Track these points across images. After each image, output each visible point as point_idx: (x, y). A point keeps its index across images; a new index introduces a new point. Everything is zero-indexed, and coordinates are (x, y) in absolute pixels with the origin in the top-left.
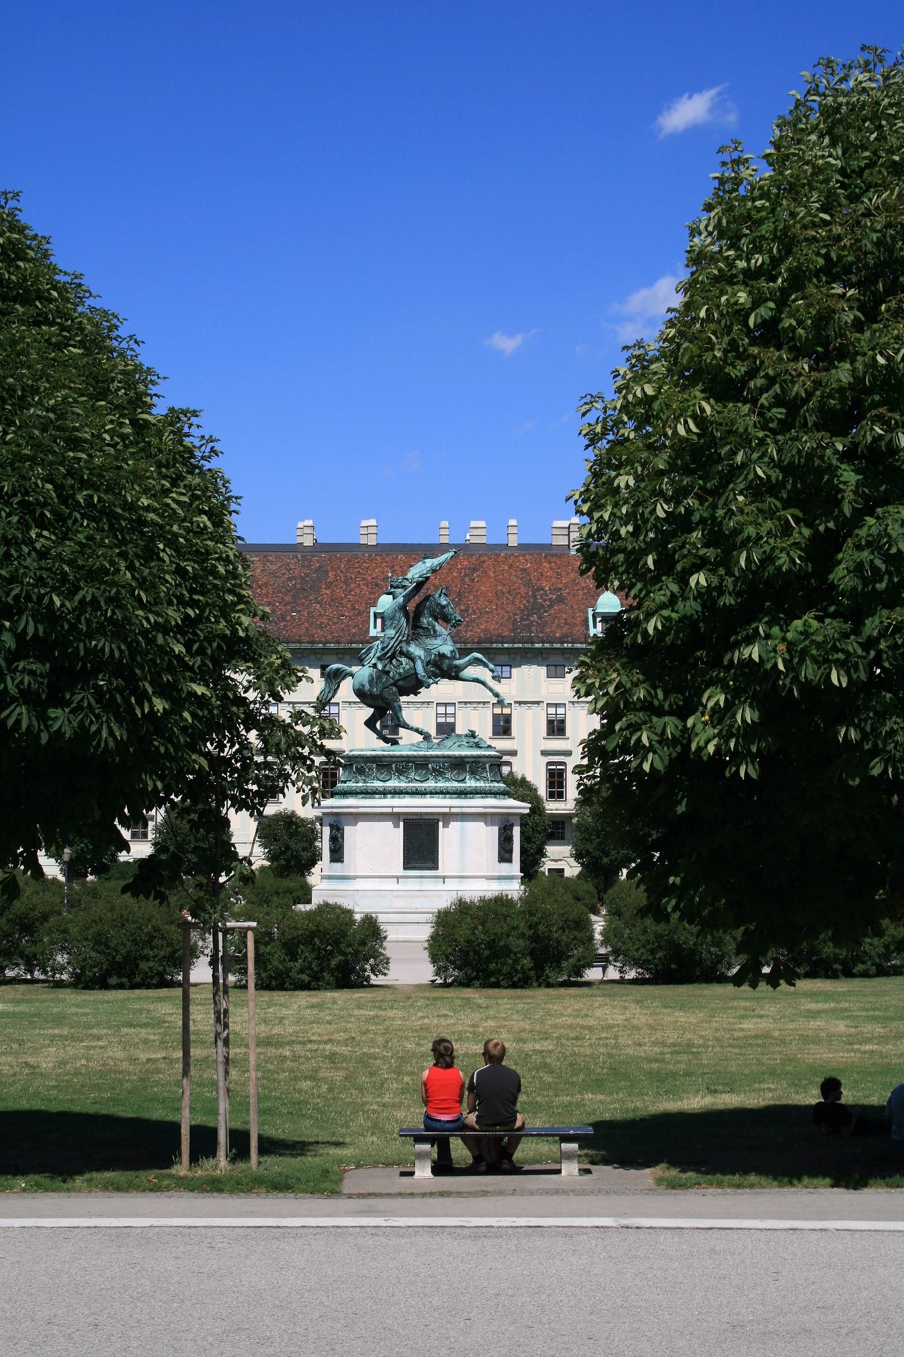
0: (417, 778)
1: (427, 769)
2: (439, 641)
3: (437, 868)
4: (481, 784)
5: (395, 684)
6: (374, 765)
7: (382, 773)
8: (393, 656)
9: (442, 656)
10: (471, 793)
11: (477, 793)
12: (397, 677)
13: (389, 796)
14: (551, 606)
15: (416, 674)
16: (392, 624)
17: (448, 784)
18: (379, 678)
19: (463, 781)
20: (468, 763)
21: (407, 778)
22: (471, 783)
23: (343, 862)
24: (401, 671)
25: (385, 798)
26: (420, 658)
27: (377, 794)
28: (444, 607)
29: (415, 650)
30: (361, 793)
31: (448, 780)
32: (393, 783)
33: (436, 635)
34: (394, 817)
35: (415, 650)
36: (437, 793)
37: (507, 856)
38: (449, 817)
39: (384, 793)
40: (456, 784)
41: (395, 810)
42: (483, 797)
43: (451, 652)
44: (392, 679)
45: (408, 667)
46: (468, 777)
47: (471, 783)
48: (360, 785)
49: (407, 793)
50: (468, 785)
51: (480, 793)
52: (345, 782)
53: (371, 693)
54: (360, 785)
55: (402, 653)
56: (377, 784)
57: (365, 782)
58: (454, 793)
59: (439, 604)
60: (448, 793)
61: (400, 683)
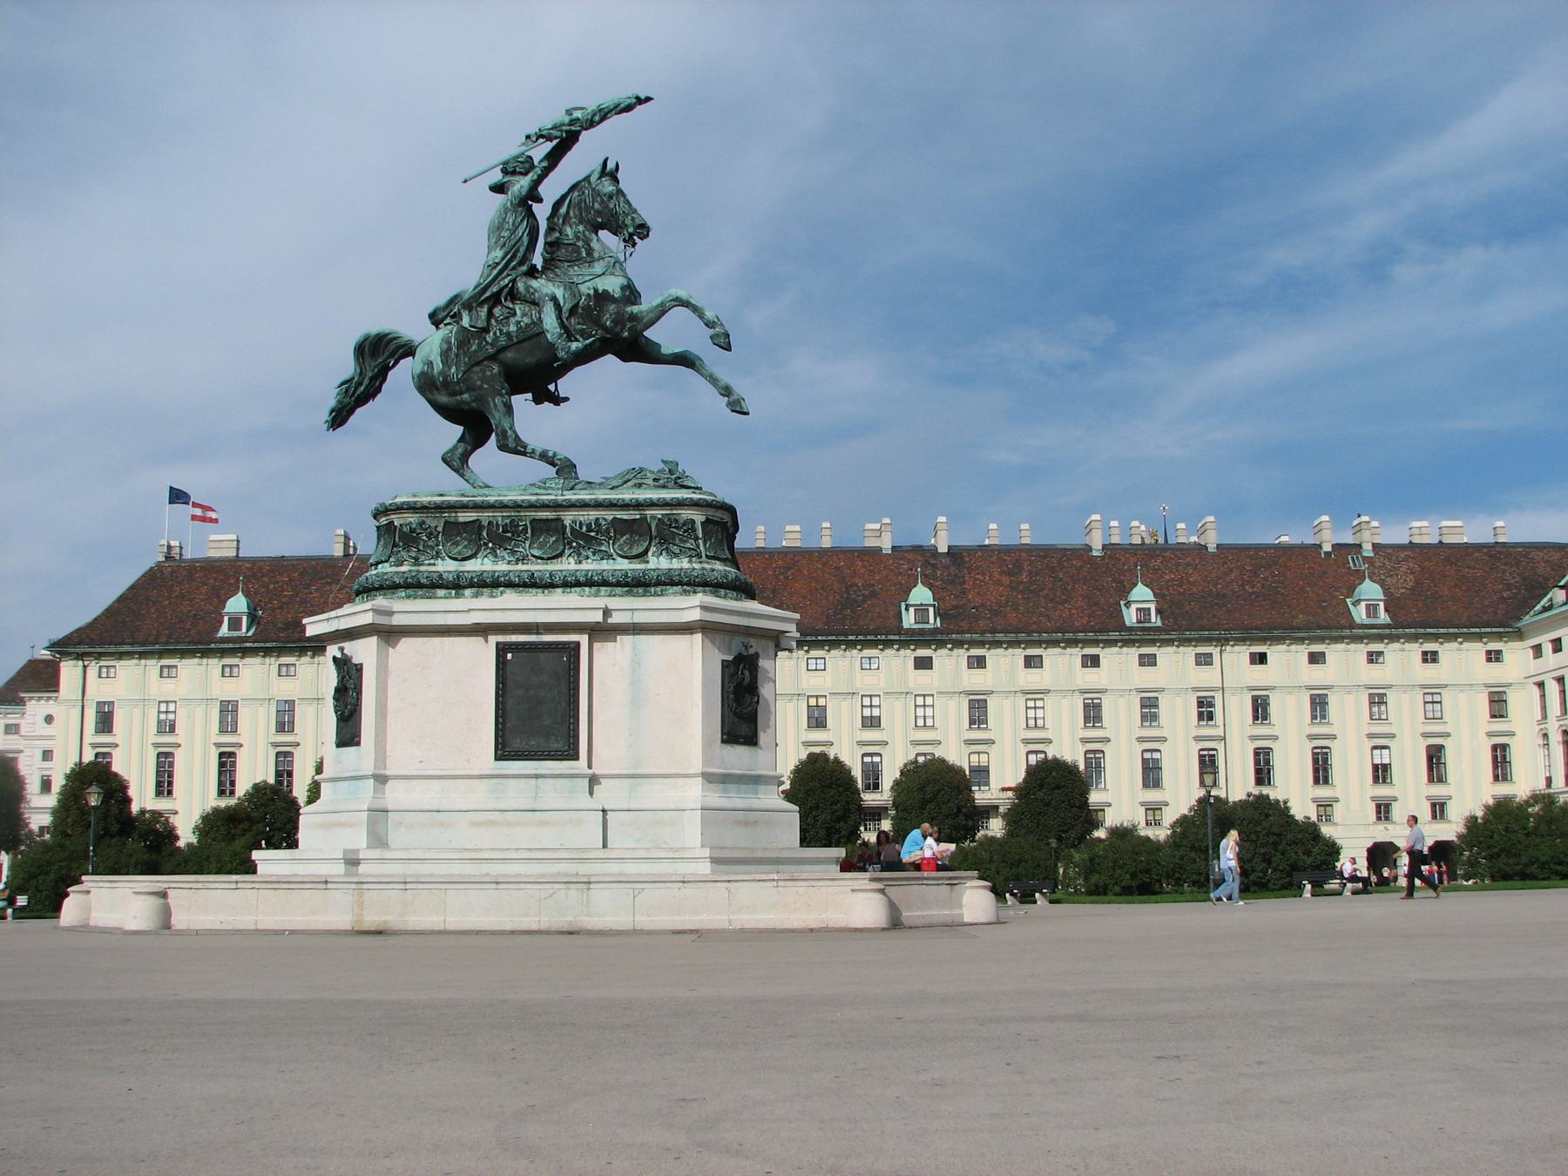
0: (537, 553)
4: (685, 564)
7: (456, 544)
9: (602, 297)
10: (659, 583)
11: (673, 584)
12: (503, 341)
13: (468, 592)
15: (542, 333)
17: (605, 565)
19: (642, 556)
21: (513, 552)
22: (659, 562)
23: (358, 744)
24: (513, 328)
25: (458, 596)
26: (554, 299)
27: (441, 587)
30: (407, 586)
32: (481, 565)
36: (578, 584)
37: (744, 729)
39: (457, 585)
40: (623, 565)
43: (623, 288)
45: (526, 320)
46: (653, 549)
47: (659, 562)
48: (404, 568)
49: (510, 585)
50: (651, 566)
51: (680, 583)
53: (445, 377)
54: (404, 568)
56: (446, 566)
57: (417, 562)
58: (618, 584)
60: (605, 583)
61: (509, 355)
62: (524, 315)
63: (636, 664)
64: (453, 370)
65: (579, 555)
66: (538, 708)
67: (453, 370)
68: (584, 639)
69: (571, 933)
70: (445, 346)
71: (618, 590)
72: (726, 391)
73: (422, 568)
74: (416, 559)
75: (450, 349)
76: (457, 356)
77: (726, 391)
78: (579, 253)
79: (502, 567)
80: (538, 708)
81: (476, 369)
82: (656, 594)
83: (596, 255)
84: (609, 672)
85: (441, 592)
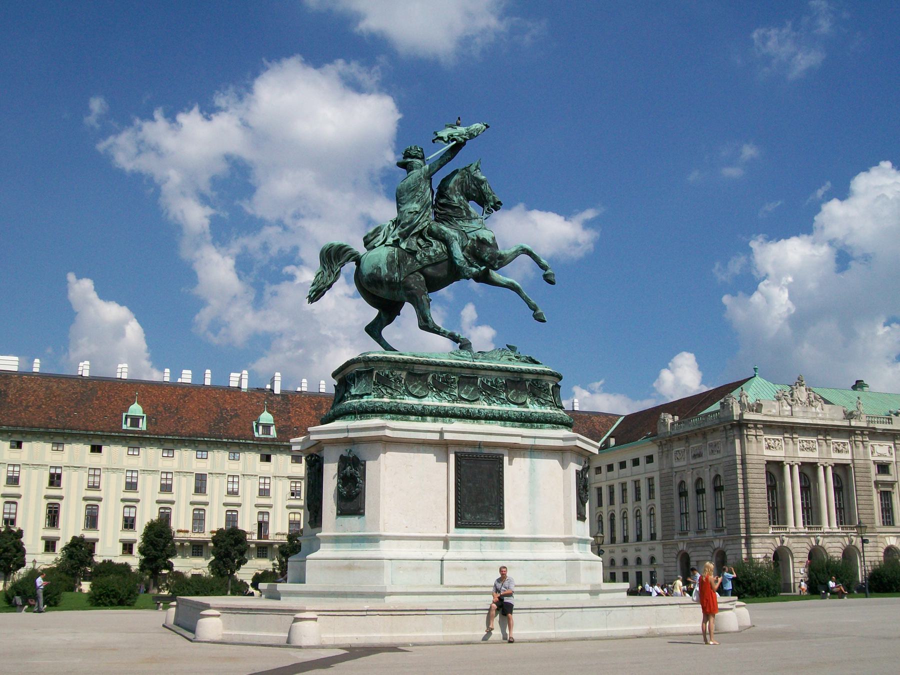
0: (463, 396)
1: (476, 384)
2: (475, 224)
3: (501, 526)
5: (421, 271)
6: (404, 375)
7: (415, 387)
8: (420, 234)
9: (482, 242)
12: (426, 262)
13: (429, 418)
14: (231, 419)
16: (414, 197)
18: (402, 260)
19: (523, 404)
20: (528, 380)
21: (450, 395)
22: (534, 408)
23: (363, 514)
24: (432, 254)
25: (424, 421)
28: (482, 182)
31: (504, 402)
32: (431, 401)
33: (469, 217)
34: (441, 446)
38: (516, 450)
39: (423, 414)
40: (515, 408)
41: (447, 436)
42: (553, 428)
44: (420, 263)
45: (439, 250)
47: (534, 408)
51: (550, 422)
52: (361, 396)
54: (386, 400)
55: (431, 233)
59: (476, 179)
62: (438, 246)
63: (532, 471)
64: (396, 275)
65: (489, 400)
66: (479, 496)
67: (396, 275)
68: (505, 452)
69: (640, 637)
70: (390, 259)
71: (517, 424)
72: (534, 308)
73: (398, 401)
74: (391, 394)
75: (393, 261)
76: (399, 266)
77: (534, 308)
78: (462, 213)
79: (446, 404)
80: (479, 496)
81: (411, 276)
82: (537, 428)
83: (473, 216)
84: (516, 474)
85: (413, 418)
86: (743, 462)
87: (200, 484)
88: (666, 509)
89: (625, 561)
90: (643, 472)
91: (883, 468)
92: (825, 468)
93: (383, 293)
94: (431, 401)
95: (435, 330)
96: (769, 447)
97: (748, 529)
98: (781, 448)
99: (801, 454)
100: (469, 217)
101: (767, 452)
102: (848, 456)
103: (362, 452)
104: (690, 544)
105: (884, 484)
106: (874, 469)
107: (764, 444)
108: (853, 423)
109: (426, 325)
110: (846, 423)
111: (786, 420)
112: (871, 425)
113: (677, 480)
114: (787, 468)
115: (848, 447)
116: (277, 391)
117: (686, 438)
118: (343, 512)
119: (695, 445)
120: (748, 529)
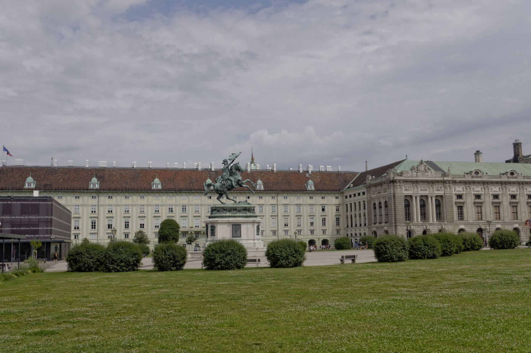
9: (239, 180)
18: (222, 186)
22: (249, 214)
29: (231, 178)
32: (228, 214)
33: (237, 174)
34: (229, 223)
35: (231, 178)
39: (226, 217)
47: (249, 214)
86: (394, 196)
87: (184, 209)
88: (369, 214)
89: (356, 234)
90: (362, 198)
91: (460, 196)
92: (431, 197)
93: (219, 192)
94: (228, 214)
95: (229, 199)
96: (406, 190)
97: (395, 222)
98: (411, 190)
99: (420, 192)
100: (237, 174)
101: (404, 192)
102: (443, 192)
103: (215, 225)
104: (377, 227)
105: (459, 203)
106: (455, 197)
107: (404, 189)
108: (445, 179)
109: (228, 198)
110: (442, 179)
111: (414, 179)
112: (454, 179)
113: (373, 203)
114: (414, 198)
115: (443, 189)
116: (213, 170)
117: (376, 185)
118: (211, 235)
119: (379, 188)
120: (395, 222)
